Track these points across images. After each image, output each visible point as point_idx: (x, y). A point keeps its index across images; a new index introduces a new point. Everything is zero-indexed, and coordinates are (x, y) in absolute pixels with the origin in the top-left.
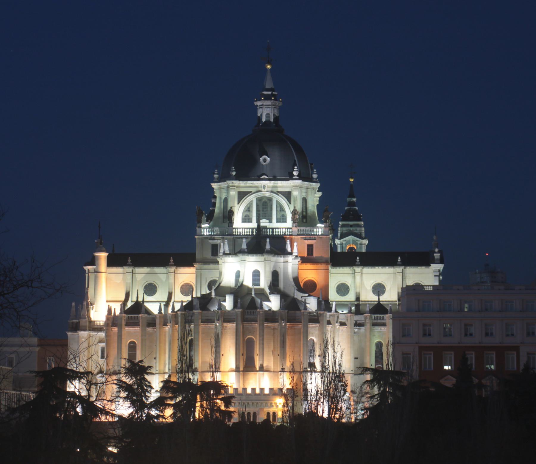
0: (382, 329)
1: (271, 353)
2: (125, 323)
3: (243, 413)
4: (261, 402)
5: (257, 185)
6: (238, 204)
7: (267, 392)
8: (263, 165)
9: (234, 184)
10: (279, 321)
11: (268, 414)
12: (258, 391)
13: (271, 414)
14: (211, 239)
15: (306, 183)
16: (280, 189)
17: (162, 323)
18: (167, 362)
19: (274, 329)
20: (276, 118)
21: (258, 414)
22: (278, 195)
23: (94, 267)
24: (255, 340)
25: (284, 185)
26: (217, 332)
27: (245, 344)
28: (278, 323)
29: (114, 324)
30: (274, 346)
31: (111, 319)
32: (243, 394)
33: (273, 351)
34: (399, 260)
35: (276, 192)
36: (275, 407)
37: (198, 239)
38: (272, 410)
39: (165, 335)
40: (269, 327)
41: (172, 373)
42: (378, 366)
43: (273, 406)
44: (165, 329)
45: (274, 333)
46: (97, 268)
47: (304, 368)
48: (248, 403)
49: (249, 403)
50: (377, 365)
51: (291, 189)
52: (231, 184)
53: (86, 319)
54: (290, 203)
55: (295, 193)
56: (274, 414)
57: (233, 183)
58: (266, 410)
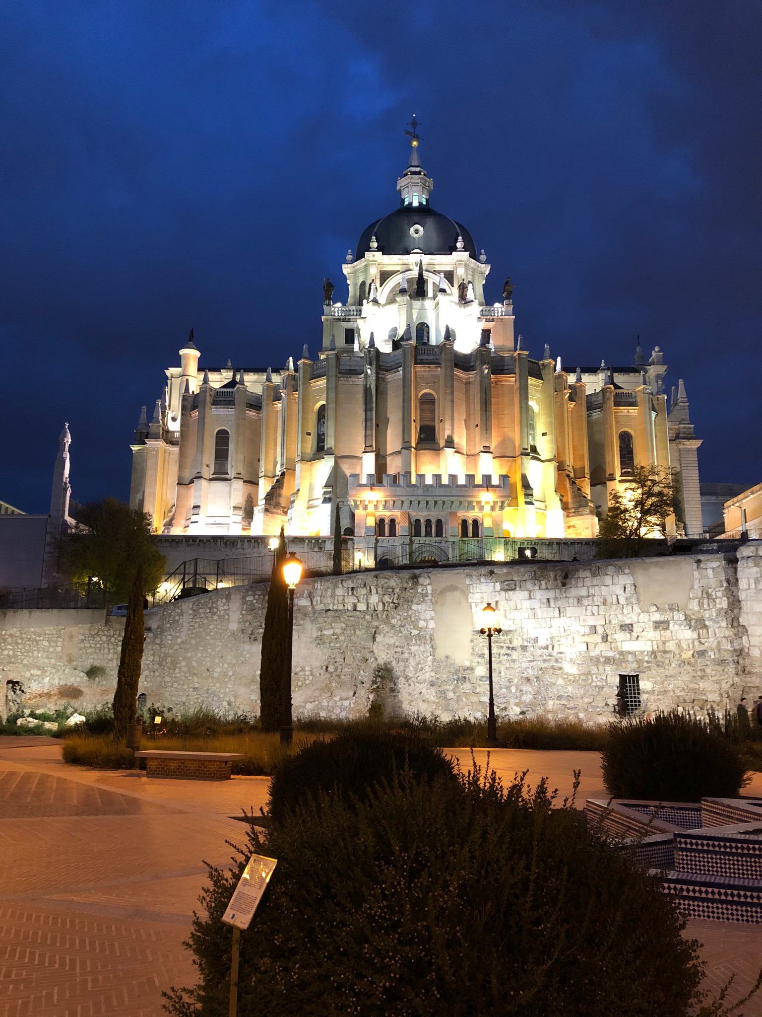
0: (631, 411)
1: (463, 423)
2: (211, 401)
3: (418, 521)
4: (452, 499)
5: (406, 262)
6: (381, 286)
7: (462, 481)
8: (414, 238)
9: (375, 259)
10: (478, 367)
11: (464, 522)
12: (445, 481)
13: (470, 522)
14: (344, 320)
15: (473, 261)
16: (437, 268)
17: (272, 398)
18: (279, 459)
19: (468, 383)
20: (427, 200)
21: (446, 523)
22: (436, 274)
23: (180, 369)
24: (436, 397)
25: (444, 262)
26: (368, 386)
27: (418, 404)
28: (476, 372)
29: (194, 407)
30: (468, 411)
31: (190, 400)
32: (419, 485)
33: (465, 420)
34: (603, 365)
35: (432, 271)
36: (477, 510)
37: (327, 320)
38: (471, 515)
39: (277, 417)
40: (460, 379)
41: (286, 469)
42: (626, 470)
43: (473, 508)
44: (277, 407)
45: (467, 390)
46: (184, 371)
47: (523, 449)
48: (427, 502)
49: (429, 503)
50: (625, 468)
51: (454, 268)
52: (371, 258)
53: (159, 422)
54: (453, 286)
55: (460, 272)
56: (475, 522)
57: (374, 256)
58: (462, 514)
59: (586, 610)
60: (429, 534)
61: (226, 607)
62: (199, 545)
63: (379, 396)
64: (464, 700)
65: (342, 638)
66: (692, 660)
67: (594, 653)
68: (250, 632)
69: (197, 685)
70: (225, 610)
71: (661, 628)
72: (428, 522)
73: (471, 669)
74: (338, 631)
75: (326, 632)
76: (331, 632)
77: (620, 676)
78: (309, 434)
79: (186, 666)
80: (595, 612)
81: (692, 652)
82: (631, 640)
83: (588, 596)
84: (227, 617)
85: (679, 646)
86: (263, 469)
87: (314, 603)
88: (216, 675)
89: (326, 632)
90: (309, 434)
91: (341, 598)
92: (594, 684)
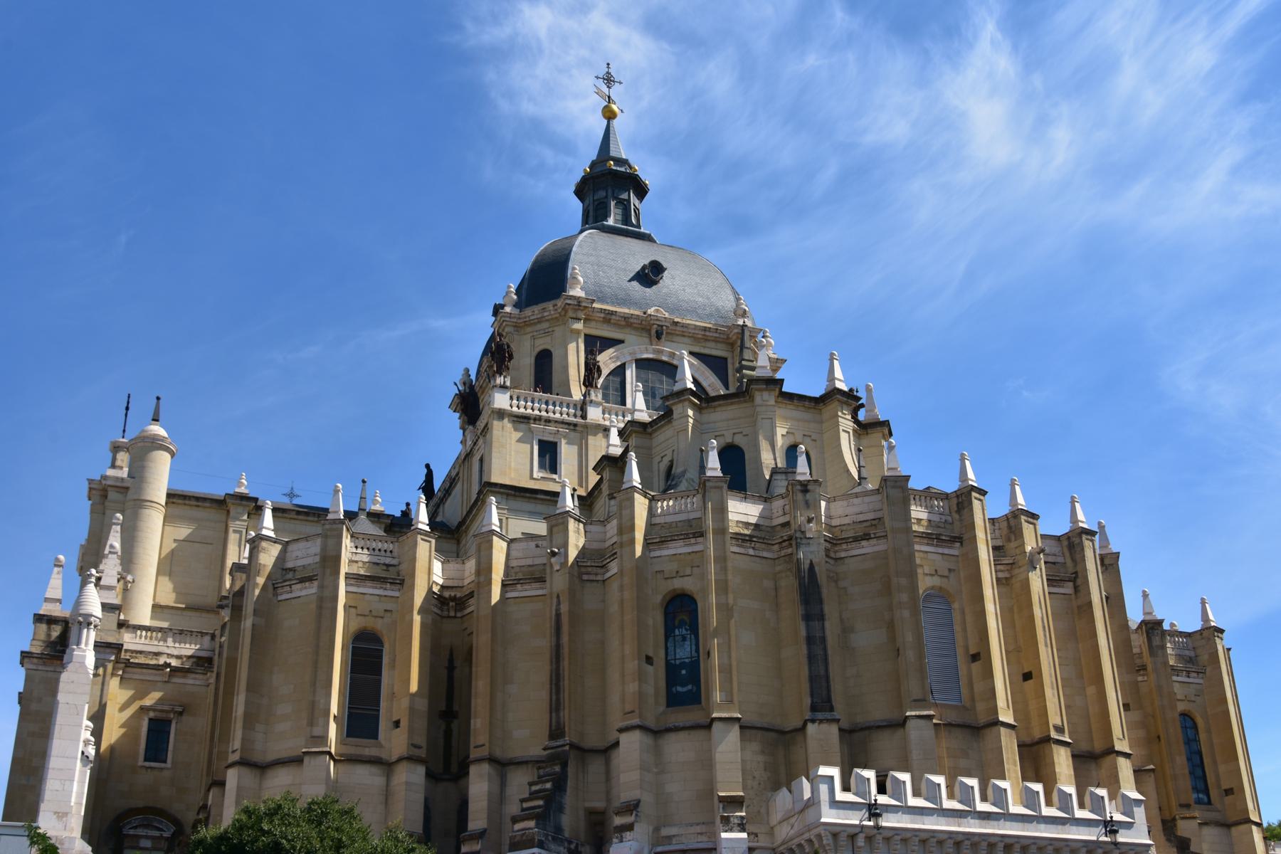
90: (649, 660)
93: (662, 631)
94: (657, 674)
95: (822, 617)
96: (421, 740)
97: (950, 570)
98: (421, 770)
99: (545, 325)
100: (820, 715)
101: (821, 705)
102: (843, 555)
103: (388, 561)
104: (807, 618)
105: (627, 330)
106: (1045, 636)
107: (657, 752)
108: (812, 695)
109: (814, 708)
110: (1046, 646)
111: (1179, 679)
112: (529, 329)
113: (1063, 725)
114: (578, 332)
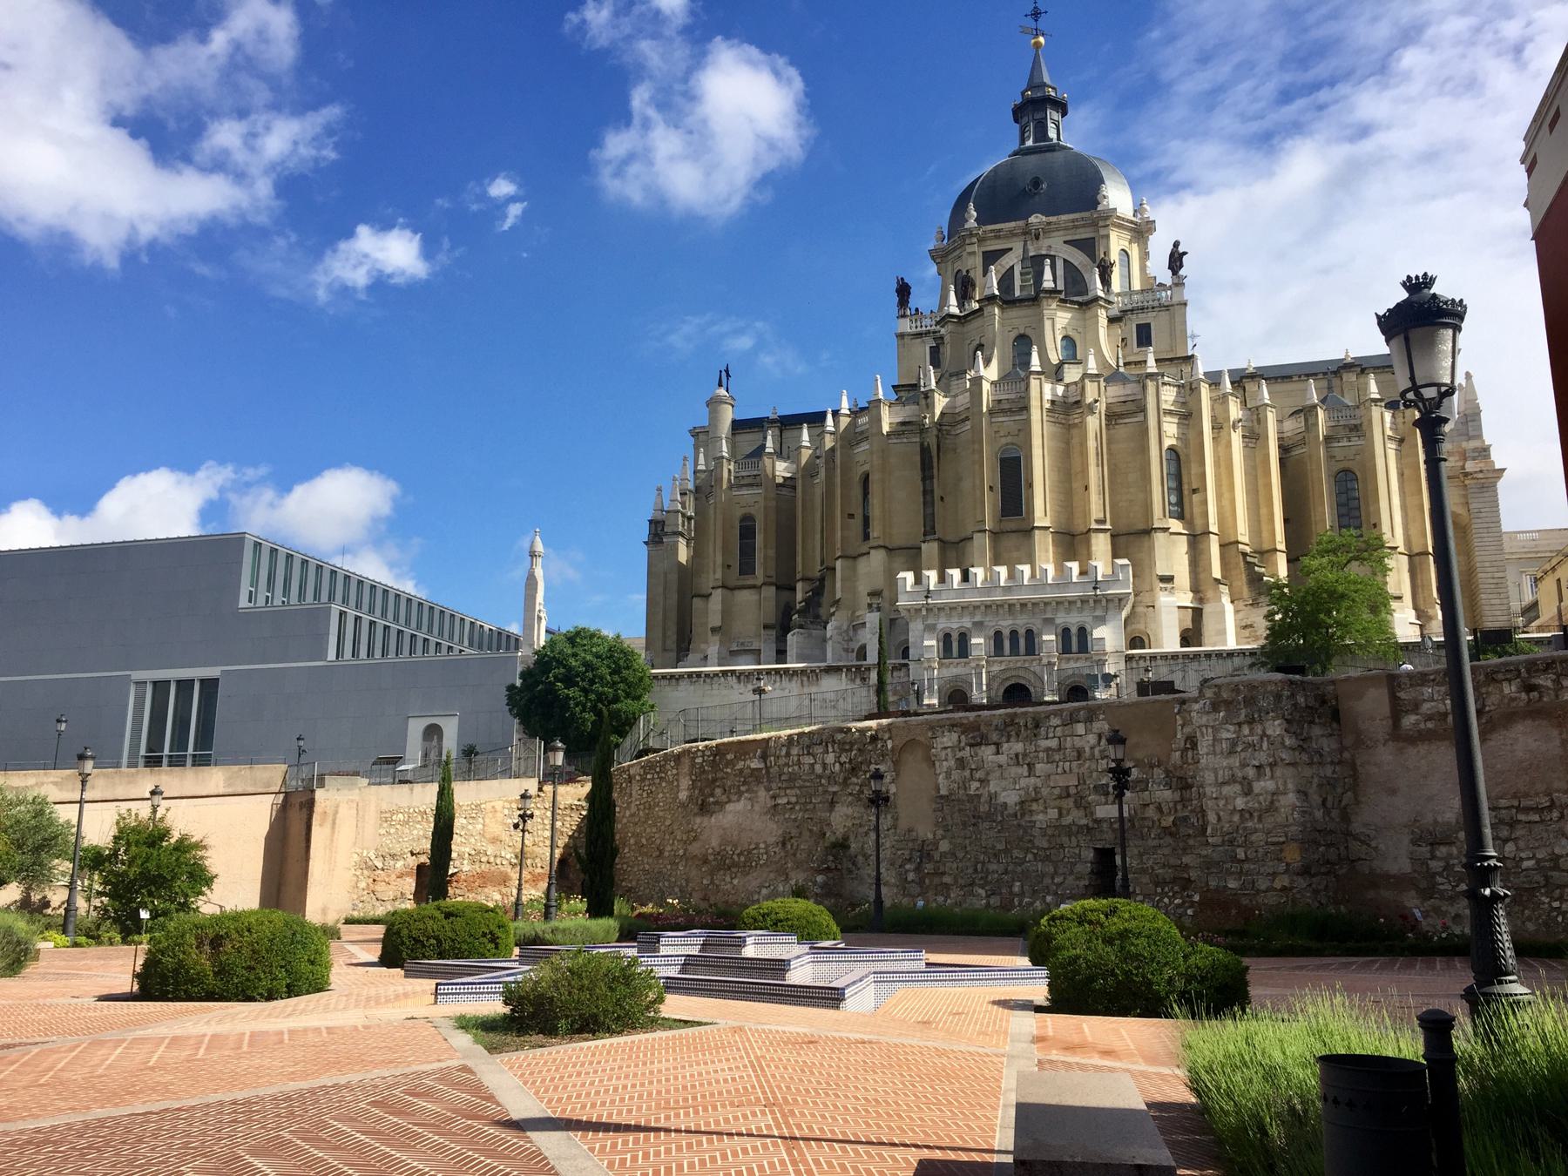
59: (1057, 766)
60: (1015, 650)
61: (675, 772)
62: (704, 681)
63: (941, 461)
64: (927, 881)
65: (797, 808)
66: (1173, 829)
67: (1067, 820)
68: (700, 802)
69: (647, 867)
70: (674, 775)
71: (1138, 789)
72: (1014, 633)
73: (936, 844)
74: (793, 800)
75: (779, 801)
76: (785, 800)
77: (1095, 849)
78: (851, 516)
79: (636, 843)
80: (1067, 769)
81: (1172, 819)
82: (1106, 803)
83: (1060, 749)
84: (675, 783)
85: (1159, 809)
86: (799, 568)
87: (768, 764)
88: (666, 854)
89: (779, 801)
90: (851, 516)
91: (796, 758)
92: (1066, 860)
93: (860, 498)
94: (857, 522)
95: (932, 478)
96: (773, 573)
97: (1019, 430)
98: (773, 589)
99: (958, 252)
100: (928, 538)
101: (929, 531)
102: (959, 431)
103: (755, 473)
104: (924, 479)
105: (1015, 239)
106: (1098, 459)
107: (854, 570)
108: (925, 526)
109: (924, 535)
110: (1098, 466)
111: (1340, 444)
112: (950, 257)
113: (1105, 517)
114: (974, 253)
